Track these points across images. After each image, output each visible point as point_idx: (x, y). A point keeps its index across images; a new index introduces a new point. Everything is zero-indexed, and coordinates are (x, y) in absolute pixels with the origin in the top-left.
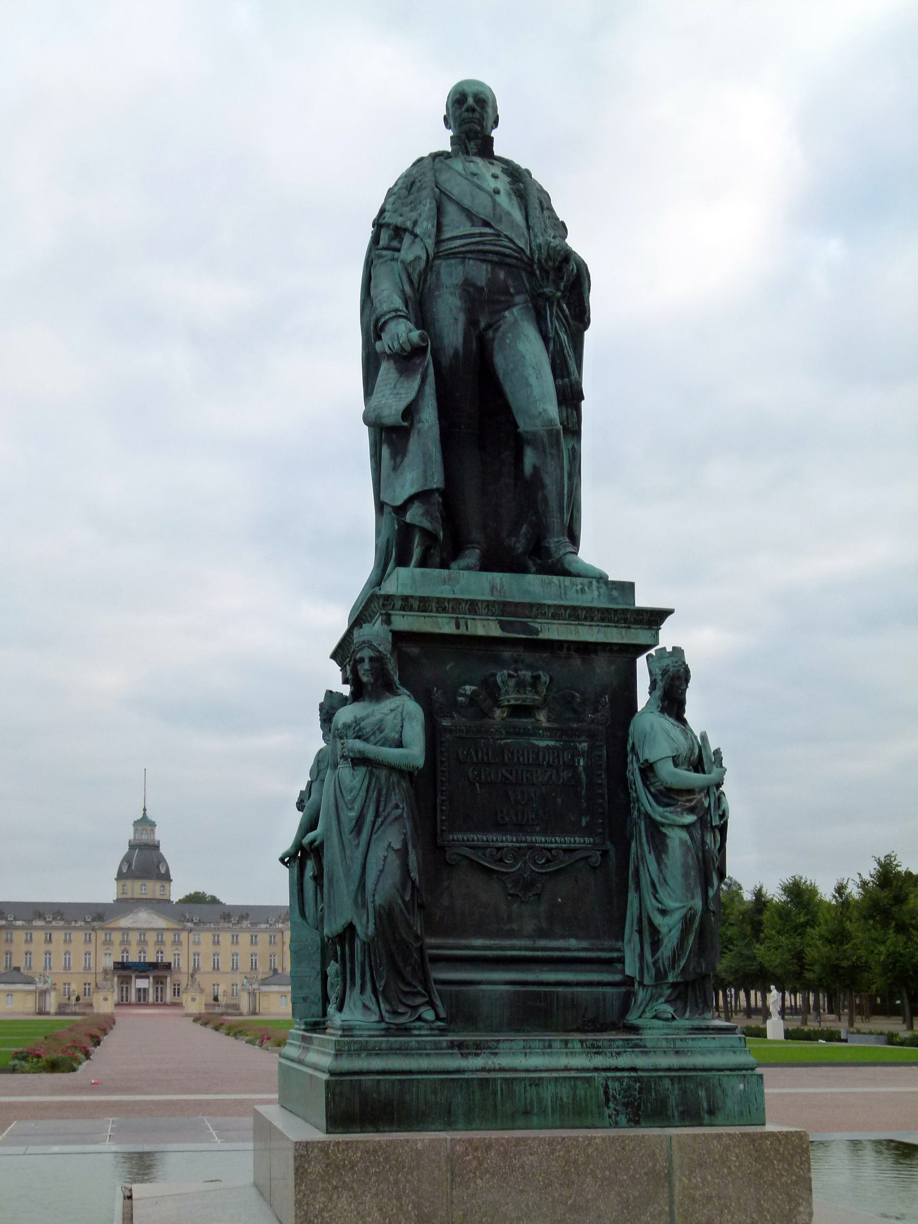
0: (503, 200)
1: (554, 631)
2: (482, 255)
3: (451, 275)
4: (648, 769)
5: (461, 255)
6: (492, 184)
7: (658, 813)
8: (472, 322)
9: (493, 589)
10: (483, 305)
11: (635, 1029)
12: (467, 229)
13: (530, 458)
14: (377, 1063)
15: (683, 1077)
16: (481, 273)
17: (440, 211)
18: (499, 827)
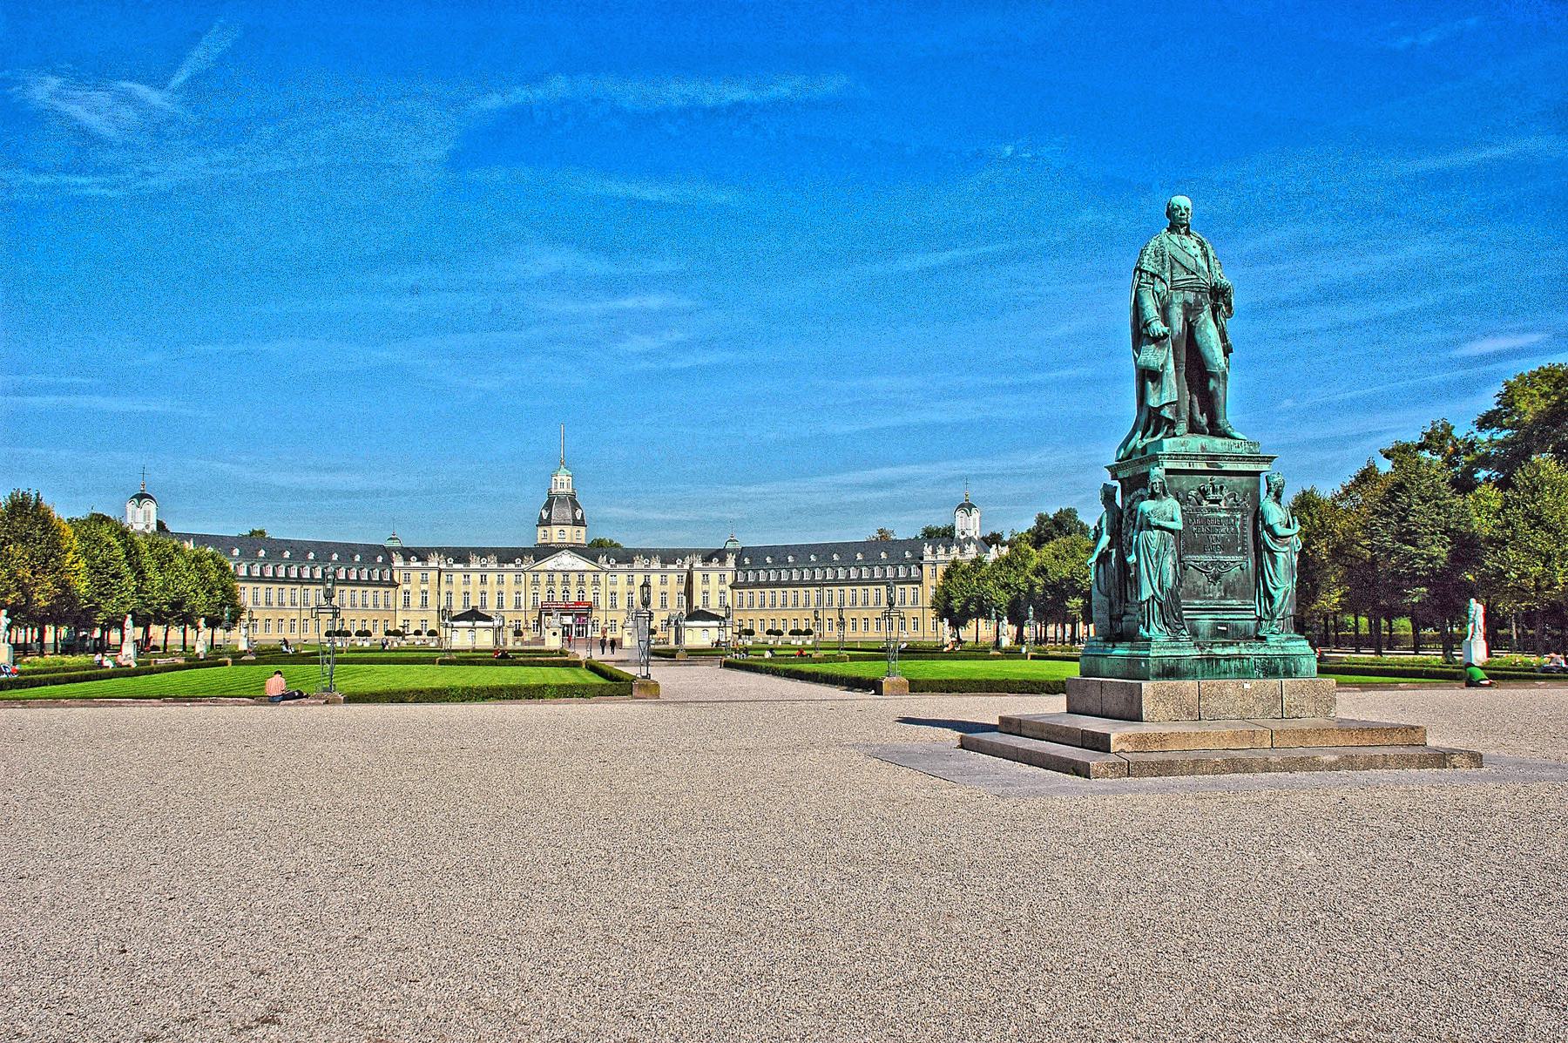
2: (1191, 289)
3: (1178, 298)
4: (1270, 529)
5: (1183, 289)
7: (1273, 546)
8: (1186, 319)
9: (1203, 448)
10: (1190, 310)
11: (1264, 638)
12: (1184, 276)
13: (1212, 384)
14: (1168, 653)
15: (1285, 657)
17: (1172, 267)
18: (1204, 552)
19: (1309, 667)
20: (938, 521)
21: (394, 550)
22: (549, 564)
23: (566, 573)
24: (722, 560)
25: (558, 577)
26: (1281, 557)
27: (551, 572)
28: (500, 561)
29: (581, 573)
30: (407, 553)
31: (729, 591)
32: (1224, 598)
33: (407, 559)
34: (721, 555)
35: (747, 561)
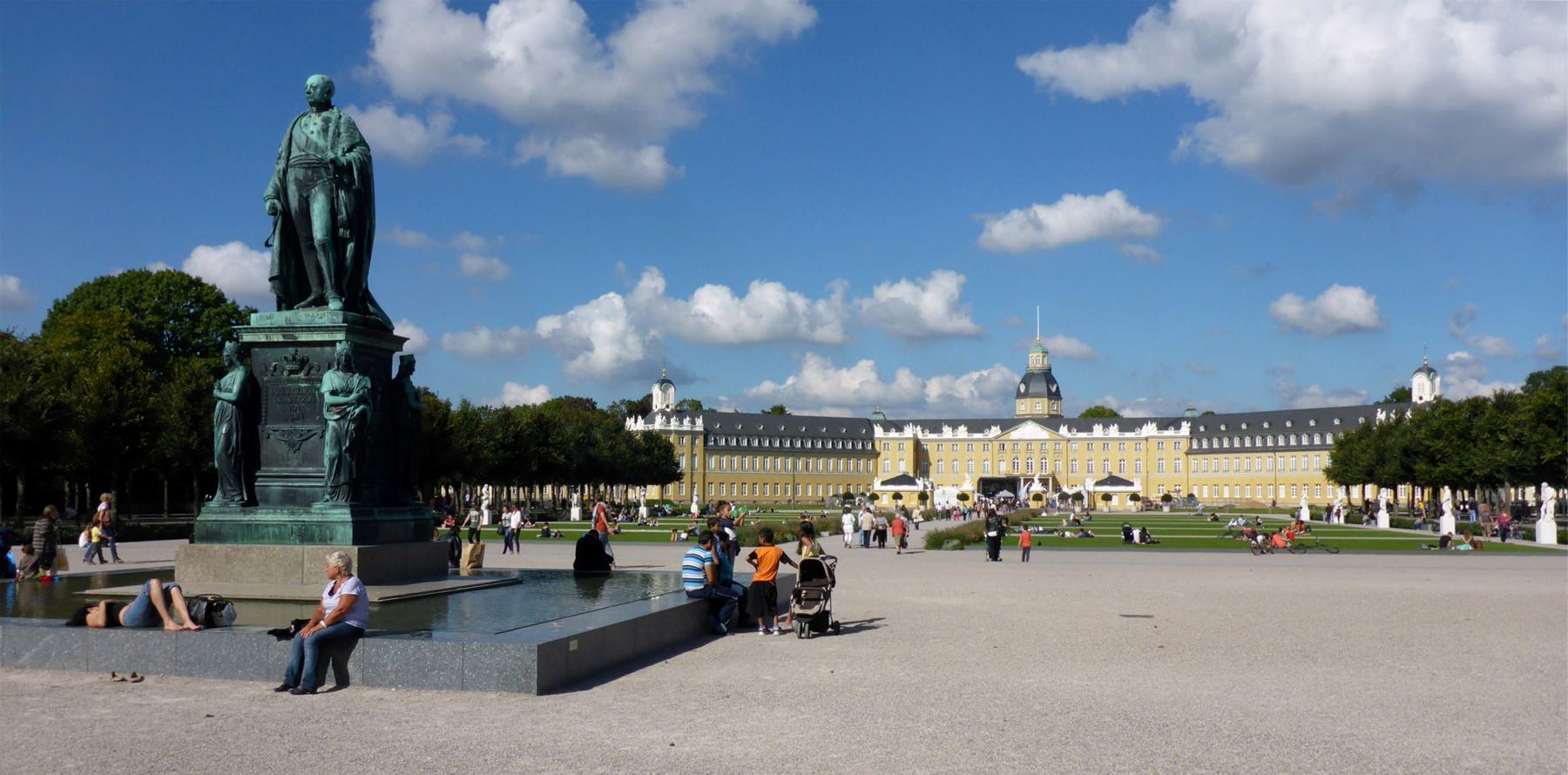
0: (314, 137)
1: (304, 337)
3: (291, 177)
6: (312, 128)
10: (305, 187)
15: (319, 524)
16: (300, 173)
19: (344, 534)
20: (636, 396)
21: (877, 422)
22: (1015, 434)
23: (1029, 442)
24: (1178, 428)
25: (1022, 446)
26: (331, 424)
27: (1016, 442)
28: (970, 431)
29: (1043, 442)
30: (887, 426)
31: (1183, 456)
32: (300, 465)
33: (886, 430)
34: (1175, 423)
35: (1202, 429)
